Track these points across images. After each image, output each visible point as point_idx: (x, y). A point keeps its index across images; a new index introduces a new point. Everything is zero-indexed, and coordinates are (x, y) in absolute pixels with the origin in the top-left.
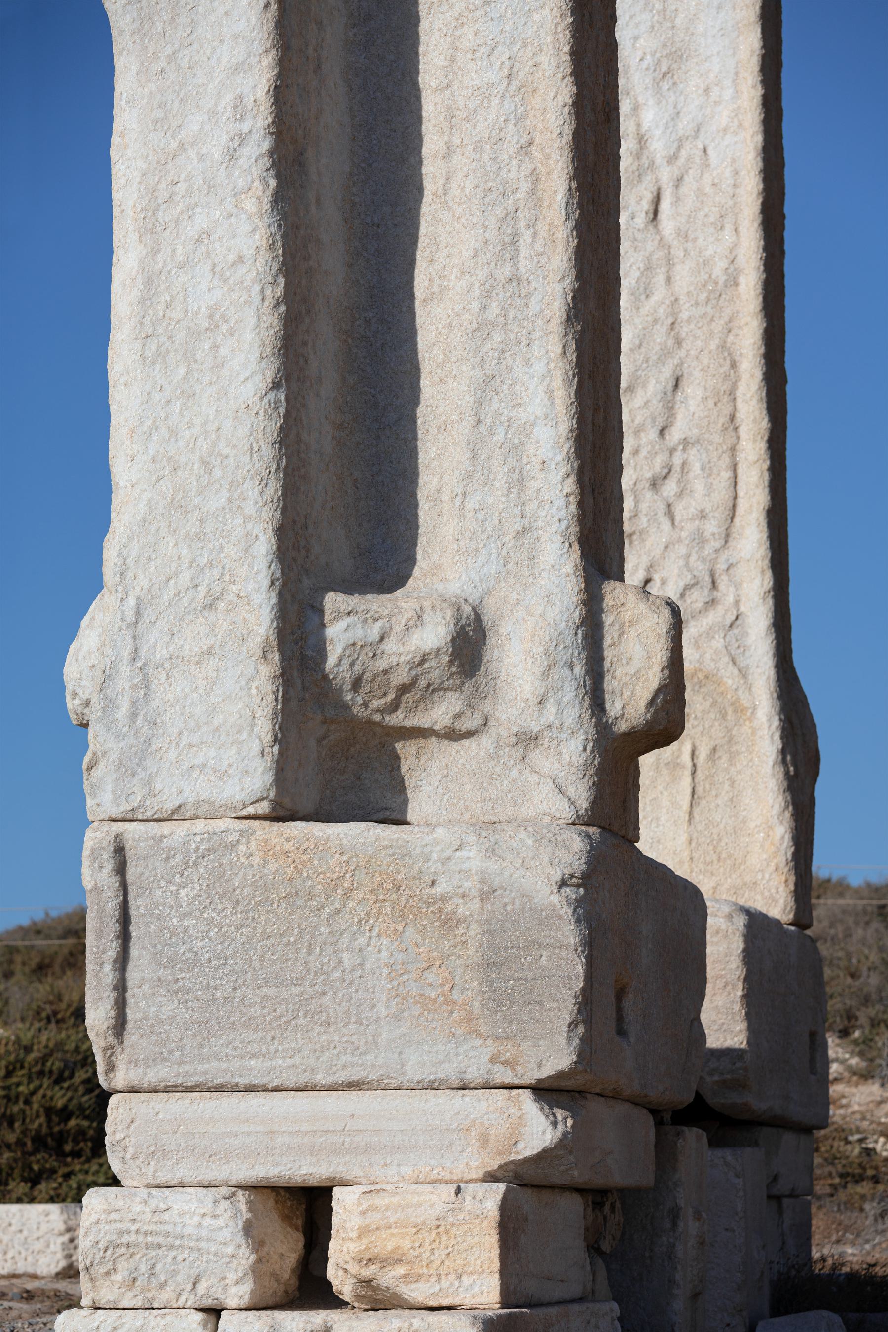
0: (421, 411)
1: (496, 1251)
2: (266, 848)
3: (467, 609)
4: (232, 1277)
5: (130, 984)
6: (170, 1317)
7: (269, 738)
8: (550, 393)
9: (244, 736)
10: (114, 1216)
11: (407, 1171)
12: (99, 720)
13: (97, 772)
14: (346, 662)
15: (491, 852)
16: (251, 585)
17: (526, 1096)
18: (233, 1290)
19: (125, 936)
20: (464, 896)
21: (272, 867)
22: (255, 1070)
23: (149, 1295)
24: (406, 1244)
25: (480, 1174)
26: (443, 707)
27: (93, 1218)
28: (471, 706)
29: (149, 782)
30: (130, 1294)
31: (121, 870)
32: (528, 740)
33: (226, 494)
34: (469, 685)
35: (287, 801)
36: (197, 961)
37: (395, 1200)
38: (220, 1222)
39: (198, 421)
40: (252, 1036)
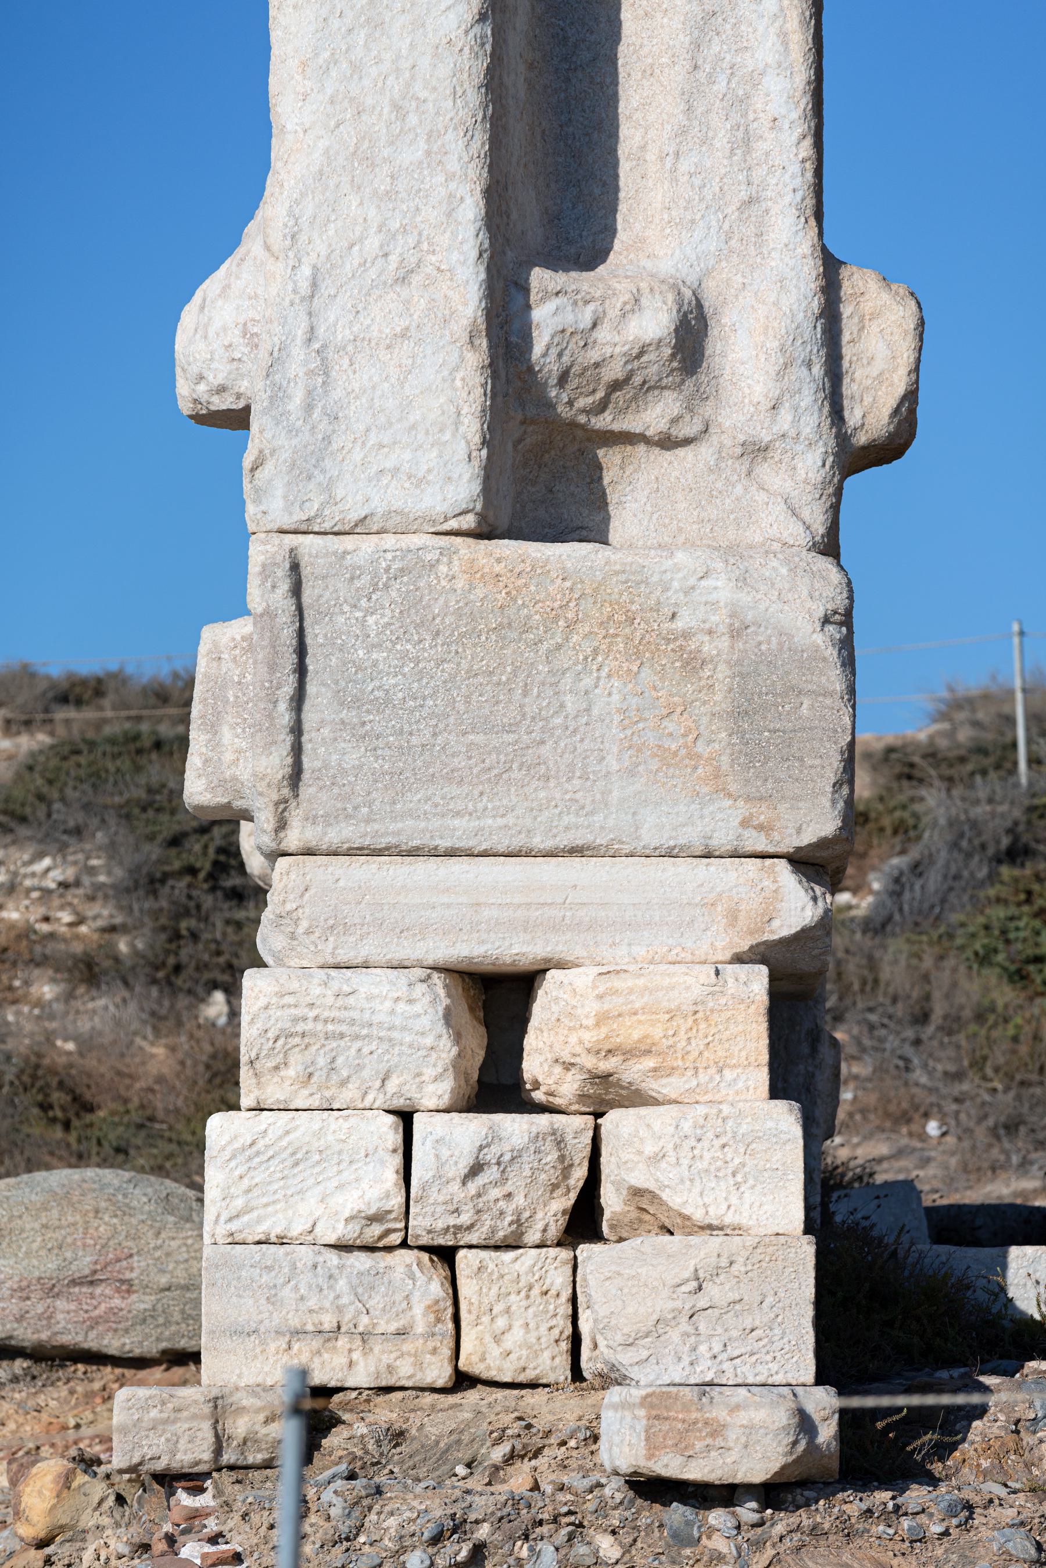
0: (622, 49)
1: (765, 1041)
2: (471, 569)
3: (688, 294)
4: (429, 1073)
5: (306, 726)
6: (355, 1119)
7: (477, 439)
8: (783, 36)
9: (447, 436)
10: (289, 1000)
11: (640, 951)
12: (265, 411)
13: (263, 474)
14: (554, 352)
15: (743, 581)
16: (455, 256)
17: (783, 867)
18: (431, 1088)
19: (301, 670)
20: (710, 632)
21: (480, 592)
22: (459, 831)
23: (328, 1094)
24: (657, 1032)
25: (728, 956)
26: (659, 409)
27: (262, 1002)
28: (690, 409)
29: (328, 488)
30: (306, 1092)
31: (296, 590)
32: (756, 451)
33: (422, 145)
34: (689, 383)
35: (491, 518)
36: (388, 701)
37: (641, 982)
38: (418, 1008)
39: (387, 56)
40: (455, 791)
